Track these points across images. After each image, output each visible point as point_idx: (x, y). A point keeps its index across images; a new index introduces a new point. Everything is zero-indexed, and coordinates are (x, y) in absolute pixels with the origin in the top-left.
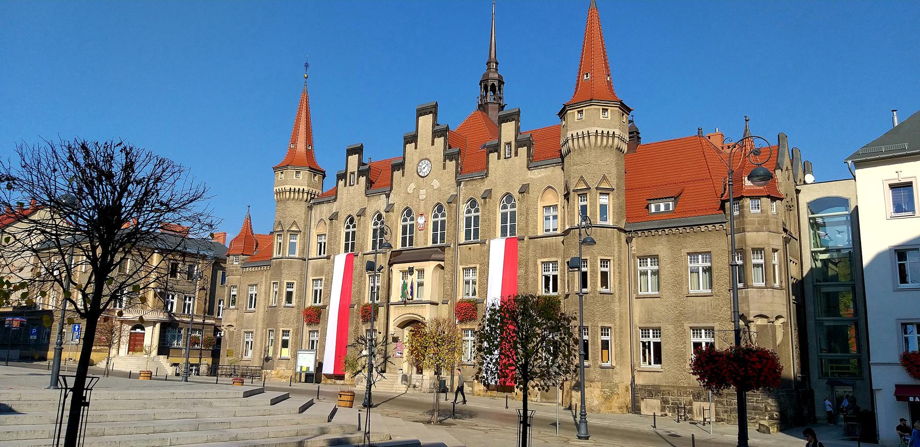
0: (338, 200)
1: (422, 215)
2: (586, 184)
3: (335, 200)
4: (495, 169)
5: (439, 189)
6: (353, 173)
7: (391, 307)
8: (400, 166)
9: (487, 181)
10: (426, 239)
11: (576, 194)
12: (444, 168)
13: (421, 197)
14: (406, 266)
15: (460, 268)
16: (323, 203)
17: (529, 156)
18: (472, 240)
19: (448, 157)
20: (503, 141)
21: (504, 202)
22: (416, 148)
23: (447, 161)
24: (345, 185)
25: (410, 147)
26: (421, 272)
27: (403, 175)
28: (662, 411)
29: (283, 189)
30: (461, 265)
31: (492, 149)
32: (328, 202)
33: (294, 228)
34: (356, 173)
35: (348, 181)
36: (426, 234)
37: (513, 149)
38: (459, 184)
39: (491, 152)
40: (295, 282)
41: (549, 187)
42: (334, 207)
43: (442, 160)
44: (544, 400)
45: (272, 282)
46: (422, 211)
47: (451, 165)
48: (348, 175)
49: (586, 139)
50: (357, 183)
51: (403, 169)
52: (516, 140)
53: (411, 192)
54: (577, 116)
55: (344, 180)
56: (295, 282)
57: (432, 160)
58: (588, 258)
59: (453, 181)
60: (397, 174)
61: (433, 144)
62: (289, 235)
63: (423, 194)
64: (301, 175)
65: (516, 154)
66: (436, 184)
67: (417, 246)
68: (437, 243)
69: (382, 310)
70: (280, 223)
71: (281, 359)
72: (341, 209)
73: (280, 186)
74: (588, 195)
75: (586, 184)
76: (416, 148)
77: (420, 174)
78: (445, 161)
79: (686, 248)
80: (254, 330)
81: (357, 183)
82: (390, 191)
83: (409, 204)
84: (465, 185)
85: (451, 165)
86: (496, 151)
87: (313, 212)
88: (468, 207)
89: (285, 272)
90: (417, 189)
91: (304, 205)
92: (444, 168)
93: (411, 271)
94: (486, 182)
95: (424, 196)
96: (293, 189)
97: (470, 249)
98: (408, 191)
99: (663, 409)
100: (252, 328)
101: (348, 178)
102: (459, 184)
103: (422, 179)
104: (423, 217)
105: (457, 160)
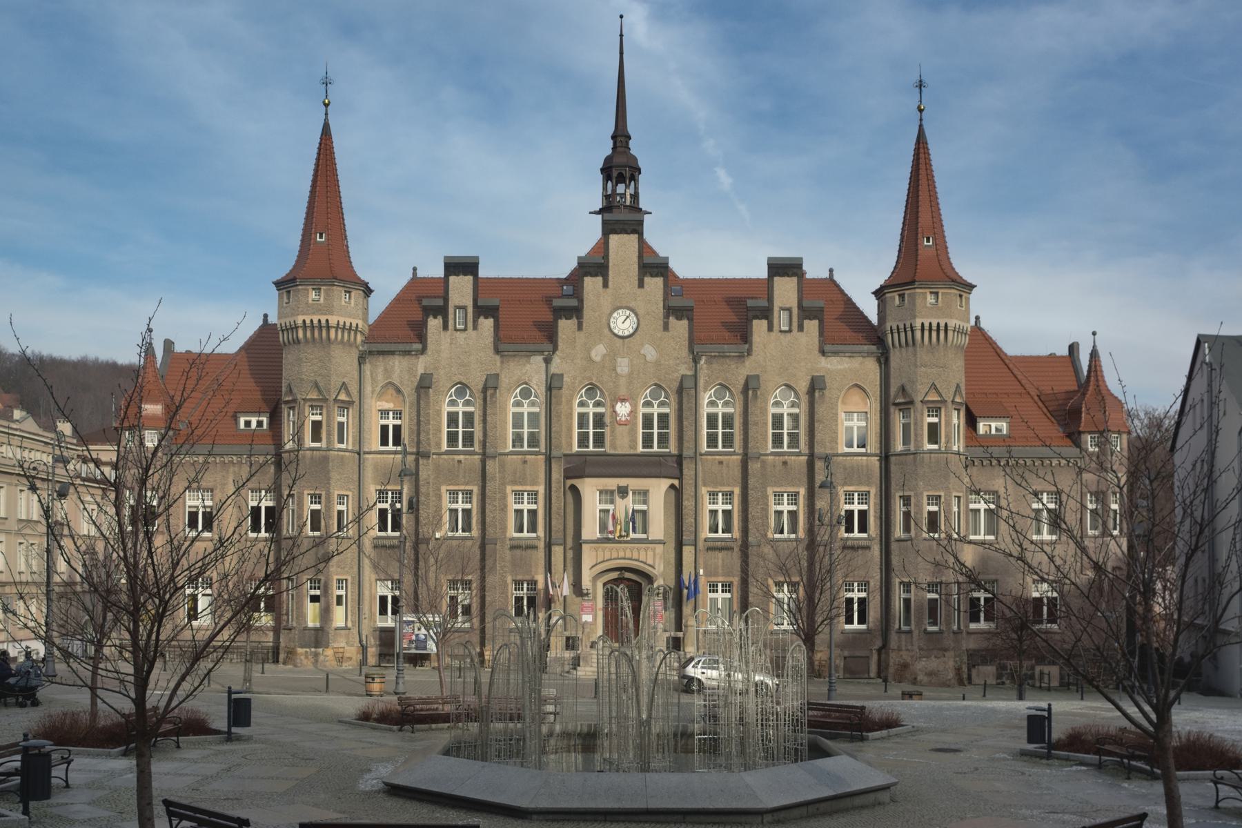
1: (623, 400)
2: (940, 395)
3: (423, 351)
4: (764, 345)
5: (657, 364)
6: (464, 308)
7: (585, 547)
8: (576, 312)
9: (749, 362)
10: (634, 441)
11: (925, 406)
12: (666, 327)
13: (619, 370)
14: (612, 483)
15: (704, 491)
16: (392, 353)
17: (821, 334)
18: (720, 448)
19: (672, 311)
20: (777, 303)
21: (776, 397)
22: (605, 285)
23: (672, 319)
24: (445, 327)
25: (591, 284)
26: (644, 495)
27: (580, 327)
28: (997, 679)
29: (323, 322)
30: (705, 486)
32: (407, 353)
33: (343, 397)
34: (470, 310)
35: (451, 323)
36: (633, 432)
37: (795, 319)
38: (696, 361)
41: (857, 385)
42: (421, 365)
43: (661, 315)
44: (848, 676)
46: (623, 392)
47: (680, 327)
48: (451, 310)
49: (934, 334)
50: (475, 328)
52: (800, 306)
53: (598, 359)
54: (930, 299)
57: (641, 312)
58: (942, 494)
59: (685, 352)
60: (566, 326)
61: (641, 284)
62: (336, 409)
63: (623, 366)
65: (801, 328)
66: (650, 352)
67: (615, 448)
68: (652, 447)
70: (317, 386)
71: (337, 629)
72: (436, 369)
73: (314, 314)
74: (943, 410)
75: (940, 395)
76: (605, 285)
77: (616, 331)
78: (667, 316)
81: (475, 328)
82: (554, 351)
83: (594, 379)
84: (708, 362)
85: (680, 327)
86: (766, 318)
87: (367, 368)
88: (710, 397)
89: (334, 475)
90: (612, 356)
91: (355, 355)
92: (666, 327)
93: (623, 492)
94: (747, 363)
96: (341, 323)
97: (721, 463)
98: (593, 354)
99: (999, 676)
101: (451, 316)
102: (696, 361)
103: (621, 341)
104: (627, 404)
105: (690, 320)
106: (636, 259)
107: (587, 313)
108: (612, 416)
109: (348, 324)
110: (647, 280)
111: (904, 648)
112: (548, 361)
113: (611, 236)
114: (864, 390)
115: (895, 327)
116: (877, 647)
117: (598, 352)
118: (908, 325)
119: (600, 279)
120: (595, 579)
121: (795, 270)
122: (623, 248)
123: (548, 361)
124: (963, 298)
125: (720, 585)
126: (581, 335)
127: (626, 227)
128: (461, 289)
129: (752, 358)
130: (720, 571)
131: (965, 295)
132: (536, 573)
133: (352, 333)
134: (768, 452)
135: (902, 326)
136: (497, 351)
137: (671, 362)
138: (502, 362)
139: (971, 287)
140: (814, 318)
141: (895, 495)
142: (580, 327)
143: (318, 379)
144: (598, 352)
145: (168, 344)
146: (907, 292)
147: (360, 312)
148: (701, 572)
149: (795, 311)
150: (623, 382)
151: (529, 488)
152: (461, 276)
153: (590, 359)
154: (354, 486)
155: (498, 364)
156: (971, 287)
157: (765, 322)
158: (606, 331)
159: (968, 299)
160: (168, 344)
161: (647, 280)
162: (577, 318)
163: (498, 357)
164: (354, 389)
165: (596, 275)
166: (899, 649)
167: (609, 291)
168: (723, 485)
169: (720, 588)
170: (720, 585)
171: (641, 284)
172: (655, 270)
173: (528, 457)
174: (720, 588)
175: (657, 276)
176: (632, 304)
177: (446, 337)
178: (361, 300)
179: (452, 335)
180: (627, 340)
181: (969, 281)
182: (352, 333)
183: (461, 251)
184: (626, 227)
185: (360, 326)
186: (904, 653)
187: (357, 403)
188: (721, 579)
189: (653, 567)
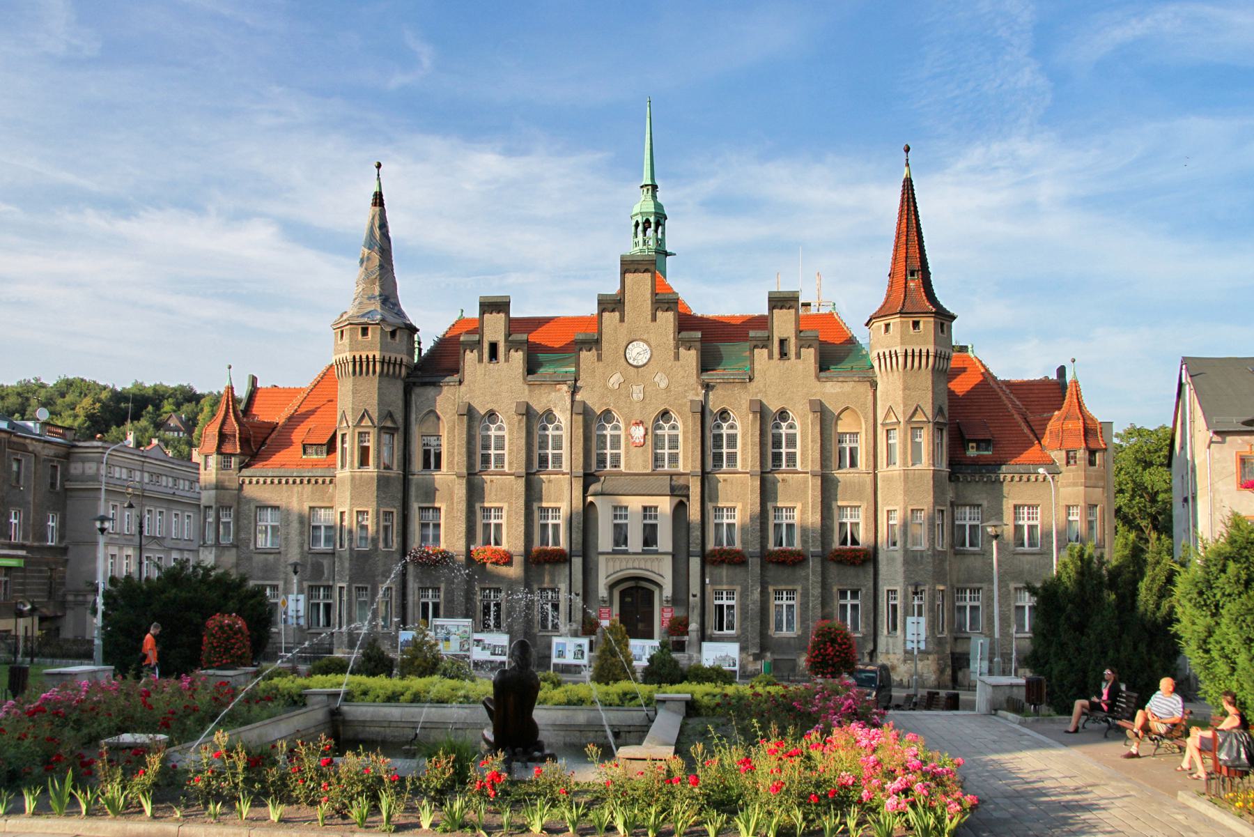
0: (466, 382)
1: (637, 424)
3: (460, 383)
8: (594, 343)
9: (752, 387)
12: (677, 357)
22: (622, 320)
24: (481, 360)
25: (610, 318)
27: (599, 358)
31: (759, 343)
33: (389, 424)
39: (756, 347)
40: (395, 510)
45: (355, 509)
46: (638, 417)
50: (507, 360)
51: (599, 349)
55: (475, 351)
56: (395, 510)
57: (653, 345)
59: (693, 379)
61: (654, 319)
64: (398, 337)
65: (798, 356)
67: (629, 469)
69: (577, 562)
73: (363, 350)
76: (622, 320)
79: (1013, 499)
80: (281, 584)
81: (507, 360)
85: (691, 357)
92: (677, 357)
95: (641, 396)
96: (387, 359)
100: (278, 579)
106: (649, 296)
107: (604, 344)
108: (627, 439)
109: (393, 359)
110: (659, 314)
111: (891, 651)
112: (574, 391)
113: (627, 275)
114: (856, 413)
115: (881, 354)
116: (868, 651)
117: (615, 380)
118: (893, 352)
119: (617, 314)
120: (611, 587)
121: (792, 303)
122: (640, 284)
123: (574, 391)
124: (945, 326)
125: (725, 593)
126: (600, 363)
127: (640, 267)
128: (495, 328)
129: (753, 384)
130: (725, 580)
131: (946, 323)
132: (559, 582)
133: (397, 367)
134: (769, 470)
135: (887, 353)
136: (524, 379)
137: (680, 388)
138: (530, 391)
139: (953, 318)
140: (809, 346)
141: (882, 510)
142: (599, 358)
143: (367, 408)
144: (615, 380)
145: (254, 380)
146: (892, 321)
147: (404, 348)
148: (707, 581)
149: (793, 341)
150: (637, 407)
151: (553, 505)
152: (494, 314)
153: (605, 386)
154: (398, 504)
155: (527, 392)
156: (953, 318)
157: (765, 351)
158: (623, 359)
159: (950, 327)
160: (254, 380)
161: (659, 314)
162: (597, 350)
163: (526, 387)
164: (400, 420)
165: (613, 311)
166: (887, 653)
167: (625, 324)
168: (727, 501)
169: (725, 596)
170: (725, 593)
171: (654, 319)
172: (667, 306)
173: (552, 476)
174: (725, 596)
175: (667, 311)
176: (645, 337)
177: (480, 369)
178: (405, 338)
179: (486, 367)
180: (640, 370)
181: (952, 311)
182: (397, 367)
183: (494, 291)
184: (640, 267)
185: (405, 361)
186: (891, 656)
187: (402, 429)
188: (725, 587)
189: (662, 576)
